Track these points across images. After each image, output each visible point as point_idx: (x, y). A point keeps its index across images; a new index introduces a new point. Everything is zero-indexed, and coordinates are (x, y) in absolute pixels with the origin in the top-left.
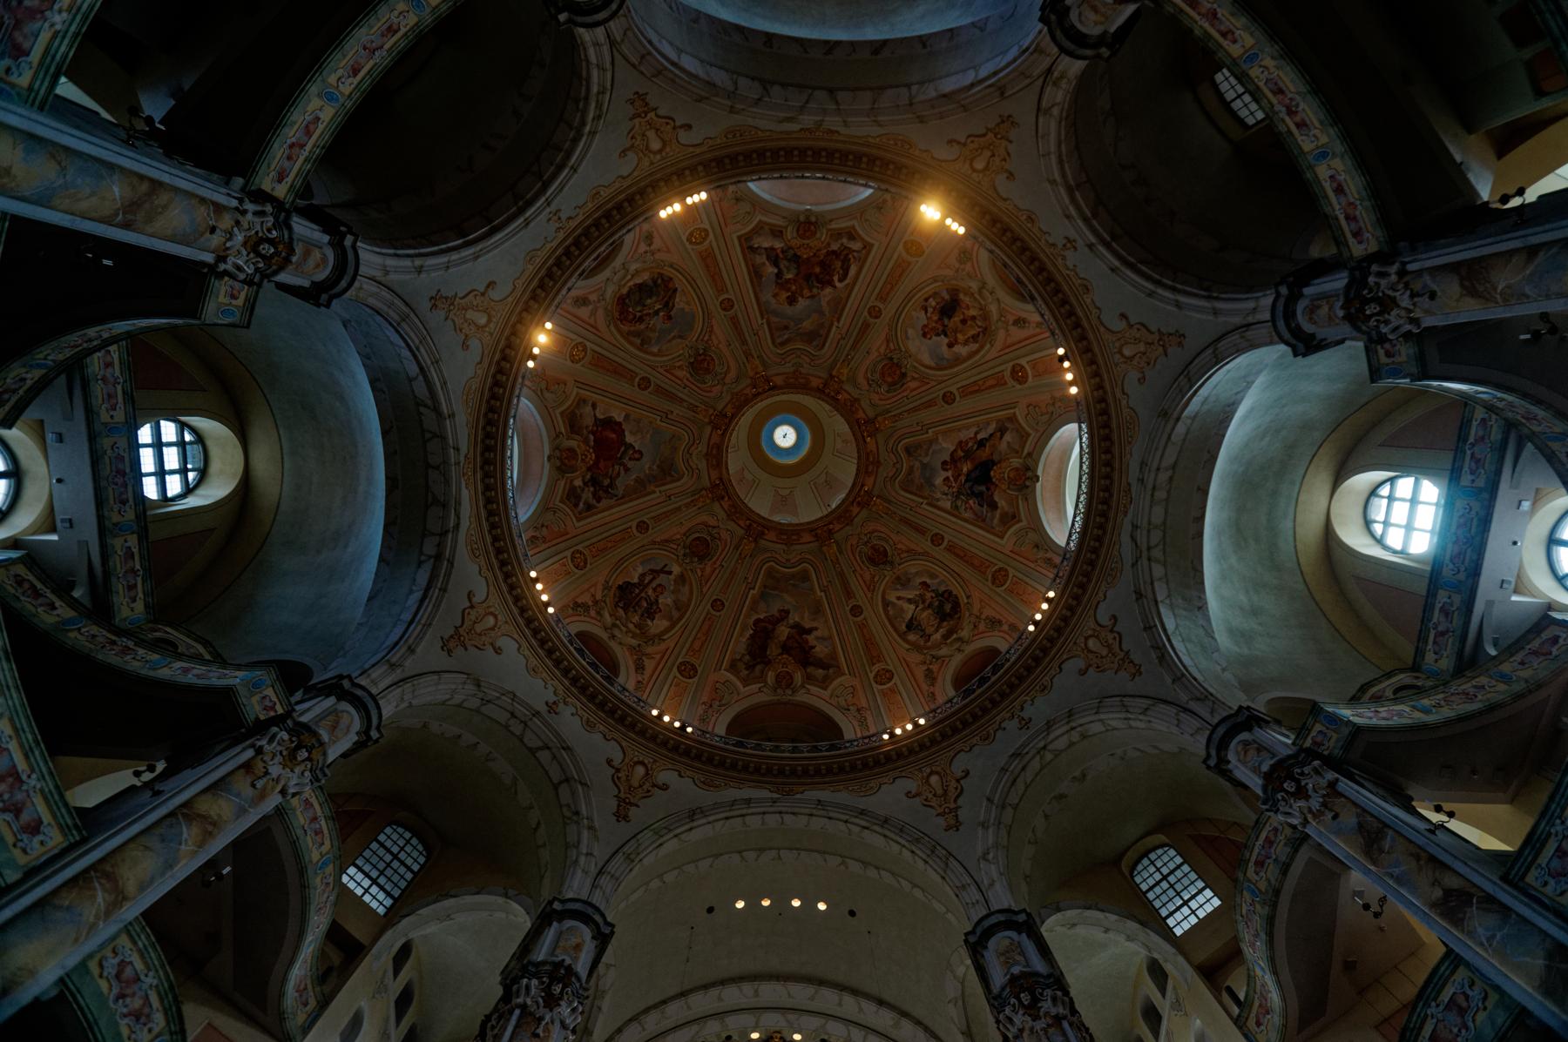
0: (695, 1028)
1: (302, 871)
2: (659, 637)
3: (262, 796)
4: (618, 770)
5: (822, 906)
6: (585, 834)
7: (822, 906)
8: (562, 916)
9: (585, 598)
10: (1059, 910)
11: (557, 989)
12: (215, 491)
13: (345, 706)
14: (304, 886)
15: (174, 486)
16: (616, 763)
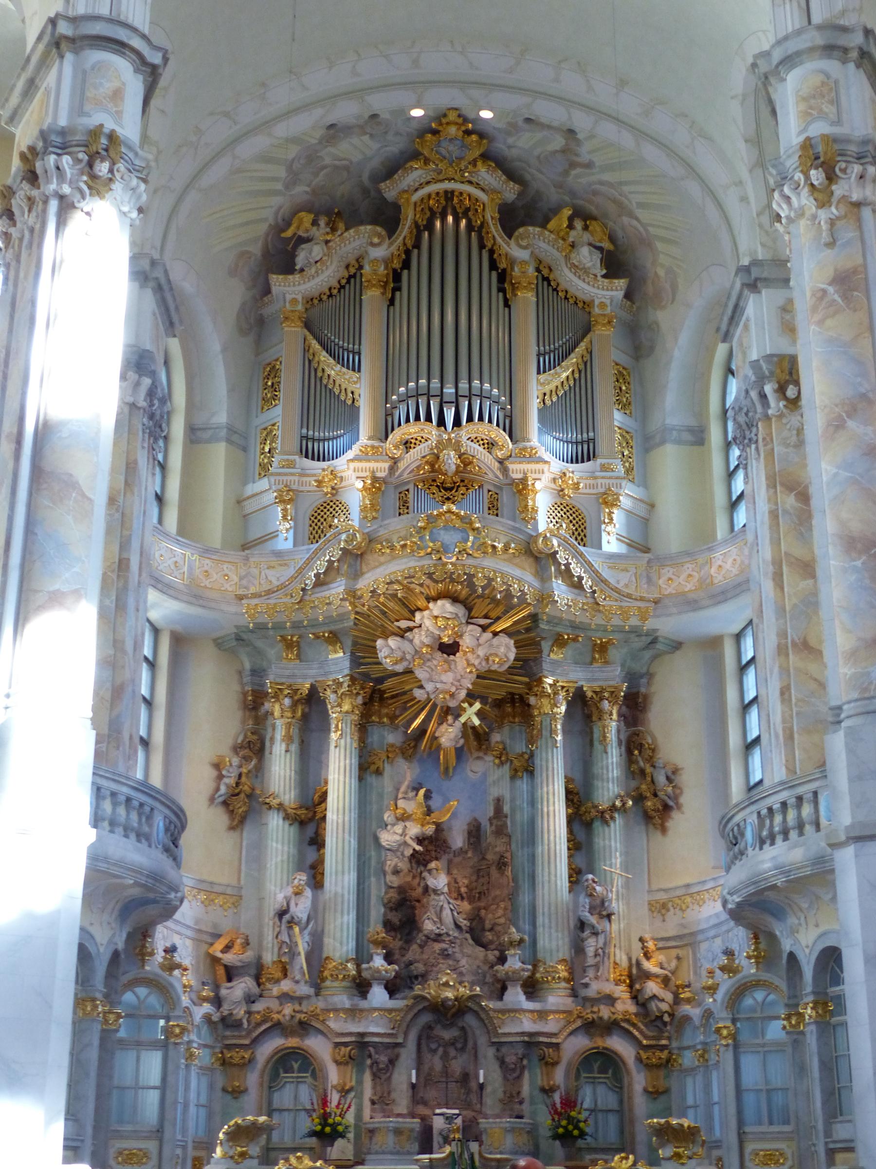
0: (318, 112)
8: (80, 43)
11: (102, 168)
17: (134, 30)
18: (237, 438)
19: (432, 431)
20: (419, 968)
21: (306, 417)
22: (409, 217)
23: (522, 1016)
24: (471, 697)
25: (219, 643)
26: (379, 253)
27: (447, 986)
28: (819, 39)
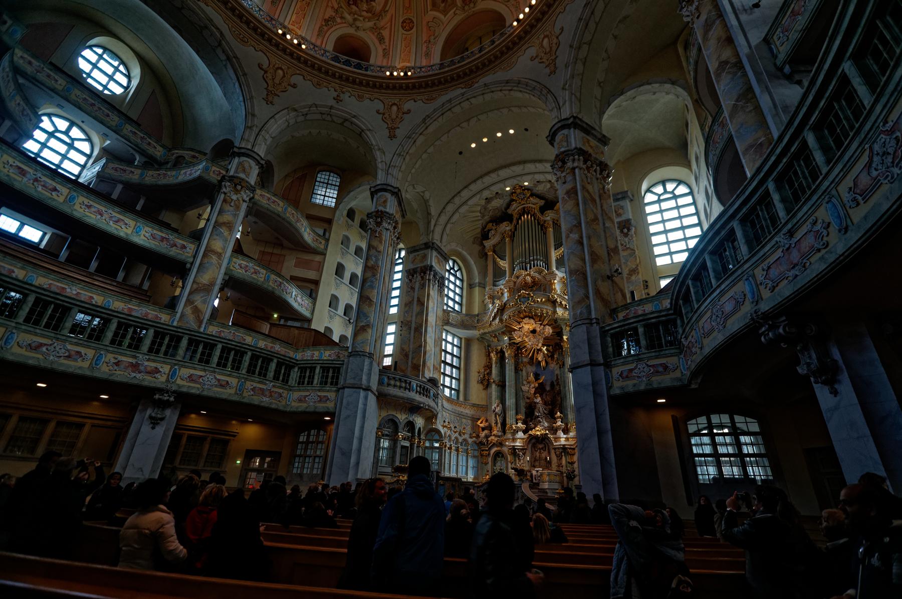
1: (279, 216)
2: (384, 10)
3: (238, 208)
4: (384, 114)
5: (512, 132)
6: (378, 153)
7: (512, 132)
8: (377, 192)
9: (330, 13)
10: (622, 94)
12: (136, 72)
13: (243, 159)
14: (284, 219)
15: (124, 81)
16: (381, 111)
17: (388, 185)
18: (482, 286)
19: (524, 273)
20: (533, 426)
21: (494, 276)
22: (515, 216)
23: (563, 439)
24: (543, 345)
25: (478, 339)
26: (508, 228)
27: (538, 431)
28: (559, 125)
